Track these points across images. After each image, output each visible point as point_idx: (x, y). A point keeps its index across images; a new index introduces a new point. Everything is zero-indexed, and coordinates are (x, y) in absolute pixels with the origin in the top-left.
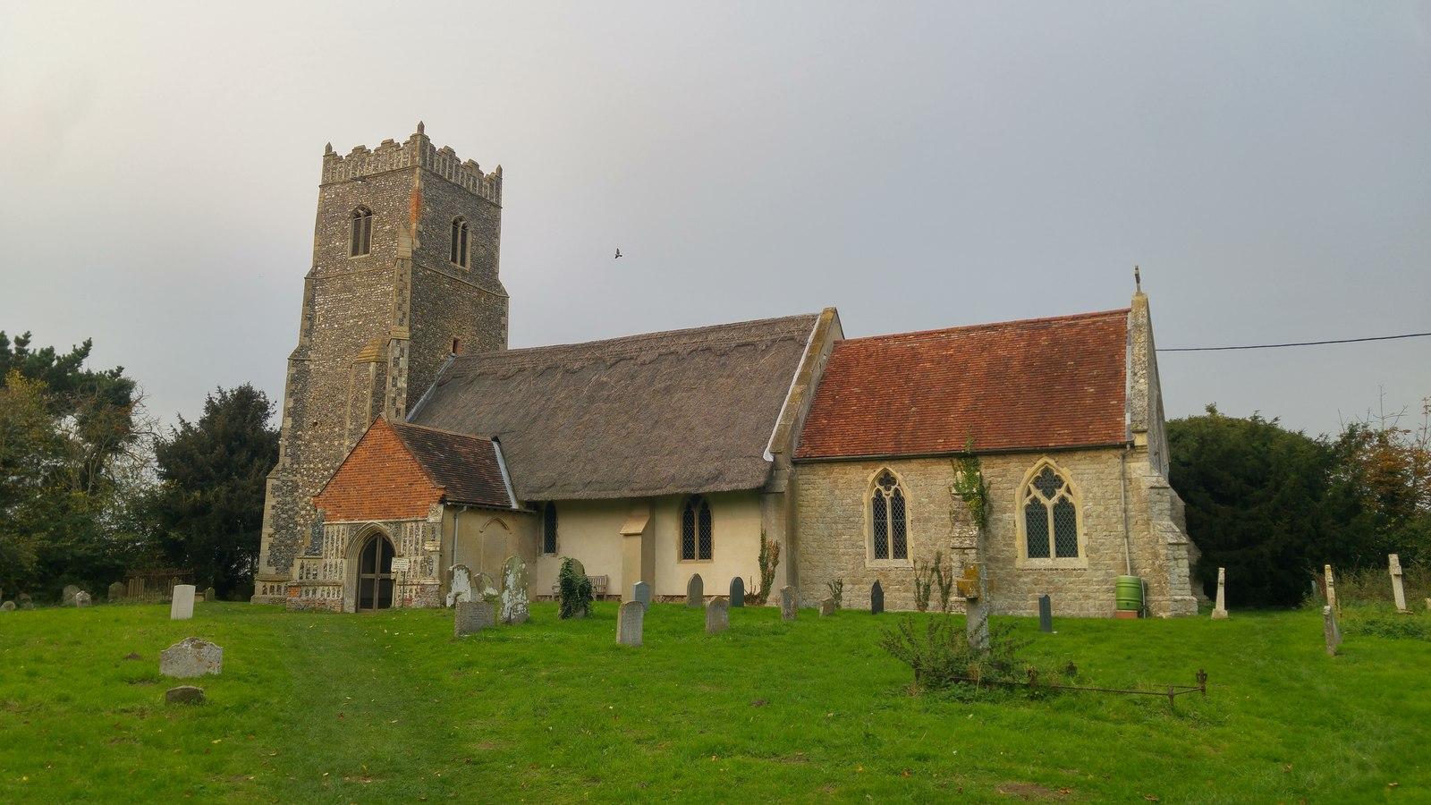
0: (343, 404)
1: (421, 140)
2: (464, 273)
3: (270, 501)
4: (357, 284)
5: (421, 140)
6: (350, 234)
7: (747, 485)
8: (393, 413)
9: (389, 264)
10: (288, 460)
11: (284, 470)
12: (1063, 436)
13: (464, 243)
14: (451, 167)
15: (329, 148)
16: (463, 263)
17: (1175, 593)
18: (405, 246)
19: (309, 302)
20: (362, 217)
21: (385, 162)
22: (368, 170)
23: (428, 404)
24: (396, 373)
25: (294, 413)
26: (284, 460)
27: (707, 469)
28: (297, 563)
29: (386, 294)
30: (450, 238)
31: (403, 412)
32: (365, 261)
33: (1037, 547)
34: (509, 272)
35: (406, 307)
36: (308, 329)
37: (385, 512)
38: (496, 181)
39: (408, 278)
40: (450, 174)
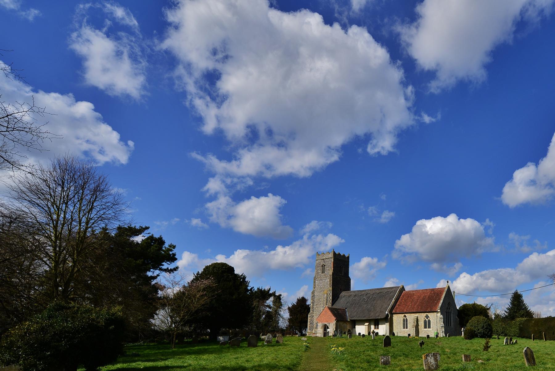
3: (309, 319)
7: (382, 318)
12: (429, 310)
17: (442, 335)
22: (324, 258)
25: (313, 303)
26: (311, 311)
27: (377, 314)
33: (425, 327)
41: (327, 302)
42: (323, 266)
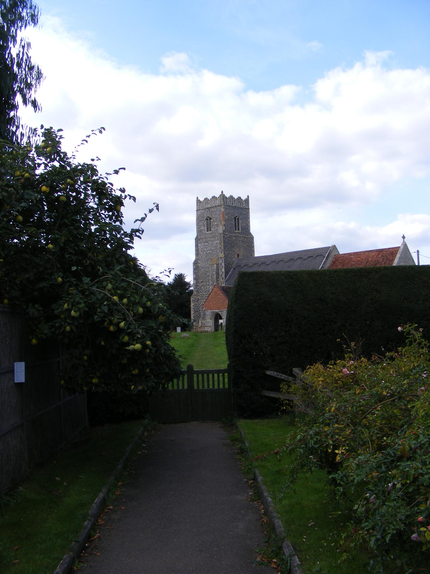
0: (209, 276)
1: (222, 195)
2: (239, 233)
3: (192, 304)
4: (209, 241)
5: (222, 195)
6: (206, 225)
8: (222, 279)
9: (217, 234)
10: (196, 292)
11: (195, 295)
13: (238, 223)
14: (232, 201)
15: (197, 198)
16: (239, 230)
18: (221, 229)
19: (197, 246)
20: (209, 219)
21: (213, 203)
22: (209, 206)
23: (231, 275)
24: (221, 267)
28: (200, 321)
29: (217, 243)
30: (234, 223)
31: (224, 278)
32: (211, 233)
34: (253, 230)
35: (223, 248)
36: (197, 254)
37: (219, 309)
38: (247, 201)
39: (222, 239)
40: (232, 204)
41: (217, 278)
42: (209, 219)
